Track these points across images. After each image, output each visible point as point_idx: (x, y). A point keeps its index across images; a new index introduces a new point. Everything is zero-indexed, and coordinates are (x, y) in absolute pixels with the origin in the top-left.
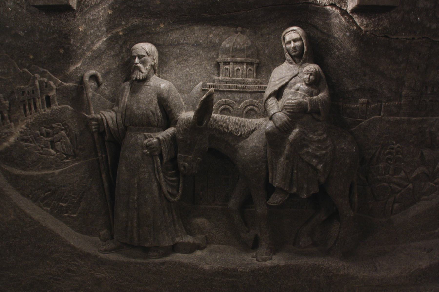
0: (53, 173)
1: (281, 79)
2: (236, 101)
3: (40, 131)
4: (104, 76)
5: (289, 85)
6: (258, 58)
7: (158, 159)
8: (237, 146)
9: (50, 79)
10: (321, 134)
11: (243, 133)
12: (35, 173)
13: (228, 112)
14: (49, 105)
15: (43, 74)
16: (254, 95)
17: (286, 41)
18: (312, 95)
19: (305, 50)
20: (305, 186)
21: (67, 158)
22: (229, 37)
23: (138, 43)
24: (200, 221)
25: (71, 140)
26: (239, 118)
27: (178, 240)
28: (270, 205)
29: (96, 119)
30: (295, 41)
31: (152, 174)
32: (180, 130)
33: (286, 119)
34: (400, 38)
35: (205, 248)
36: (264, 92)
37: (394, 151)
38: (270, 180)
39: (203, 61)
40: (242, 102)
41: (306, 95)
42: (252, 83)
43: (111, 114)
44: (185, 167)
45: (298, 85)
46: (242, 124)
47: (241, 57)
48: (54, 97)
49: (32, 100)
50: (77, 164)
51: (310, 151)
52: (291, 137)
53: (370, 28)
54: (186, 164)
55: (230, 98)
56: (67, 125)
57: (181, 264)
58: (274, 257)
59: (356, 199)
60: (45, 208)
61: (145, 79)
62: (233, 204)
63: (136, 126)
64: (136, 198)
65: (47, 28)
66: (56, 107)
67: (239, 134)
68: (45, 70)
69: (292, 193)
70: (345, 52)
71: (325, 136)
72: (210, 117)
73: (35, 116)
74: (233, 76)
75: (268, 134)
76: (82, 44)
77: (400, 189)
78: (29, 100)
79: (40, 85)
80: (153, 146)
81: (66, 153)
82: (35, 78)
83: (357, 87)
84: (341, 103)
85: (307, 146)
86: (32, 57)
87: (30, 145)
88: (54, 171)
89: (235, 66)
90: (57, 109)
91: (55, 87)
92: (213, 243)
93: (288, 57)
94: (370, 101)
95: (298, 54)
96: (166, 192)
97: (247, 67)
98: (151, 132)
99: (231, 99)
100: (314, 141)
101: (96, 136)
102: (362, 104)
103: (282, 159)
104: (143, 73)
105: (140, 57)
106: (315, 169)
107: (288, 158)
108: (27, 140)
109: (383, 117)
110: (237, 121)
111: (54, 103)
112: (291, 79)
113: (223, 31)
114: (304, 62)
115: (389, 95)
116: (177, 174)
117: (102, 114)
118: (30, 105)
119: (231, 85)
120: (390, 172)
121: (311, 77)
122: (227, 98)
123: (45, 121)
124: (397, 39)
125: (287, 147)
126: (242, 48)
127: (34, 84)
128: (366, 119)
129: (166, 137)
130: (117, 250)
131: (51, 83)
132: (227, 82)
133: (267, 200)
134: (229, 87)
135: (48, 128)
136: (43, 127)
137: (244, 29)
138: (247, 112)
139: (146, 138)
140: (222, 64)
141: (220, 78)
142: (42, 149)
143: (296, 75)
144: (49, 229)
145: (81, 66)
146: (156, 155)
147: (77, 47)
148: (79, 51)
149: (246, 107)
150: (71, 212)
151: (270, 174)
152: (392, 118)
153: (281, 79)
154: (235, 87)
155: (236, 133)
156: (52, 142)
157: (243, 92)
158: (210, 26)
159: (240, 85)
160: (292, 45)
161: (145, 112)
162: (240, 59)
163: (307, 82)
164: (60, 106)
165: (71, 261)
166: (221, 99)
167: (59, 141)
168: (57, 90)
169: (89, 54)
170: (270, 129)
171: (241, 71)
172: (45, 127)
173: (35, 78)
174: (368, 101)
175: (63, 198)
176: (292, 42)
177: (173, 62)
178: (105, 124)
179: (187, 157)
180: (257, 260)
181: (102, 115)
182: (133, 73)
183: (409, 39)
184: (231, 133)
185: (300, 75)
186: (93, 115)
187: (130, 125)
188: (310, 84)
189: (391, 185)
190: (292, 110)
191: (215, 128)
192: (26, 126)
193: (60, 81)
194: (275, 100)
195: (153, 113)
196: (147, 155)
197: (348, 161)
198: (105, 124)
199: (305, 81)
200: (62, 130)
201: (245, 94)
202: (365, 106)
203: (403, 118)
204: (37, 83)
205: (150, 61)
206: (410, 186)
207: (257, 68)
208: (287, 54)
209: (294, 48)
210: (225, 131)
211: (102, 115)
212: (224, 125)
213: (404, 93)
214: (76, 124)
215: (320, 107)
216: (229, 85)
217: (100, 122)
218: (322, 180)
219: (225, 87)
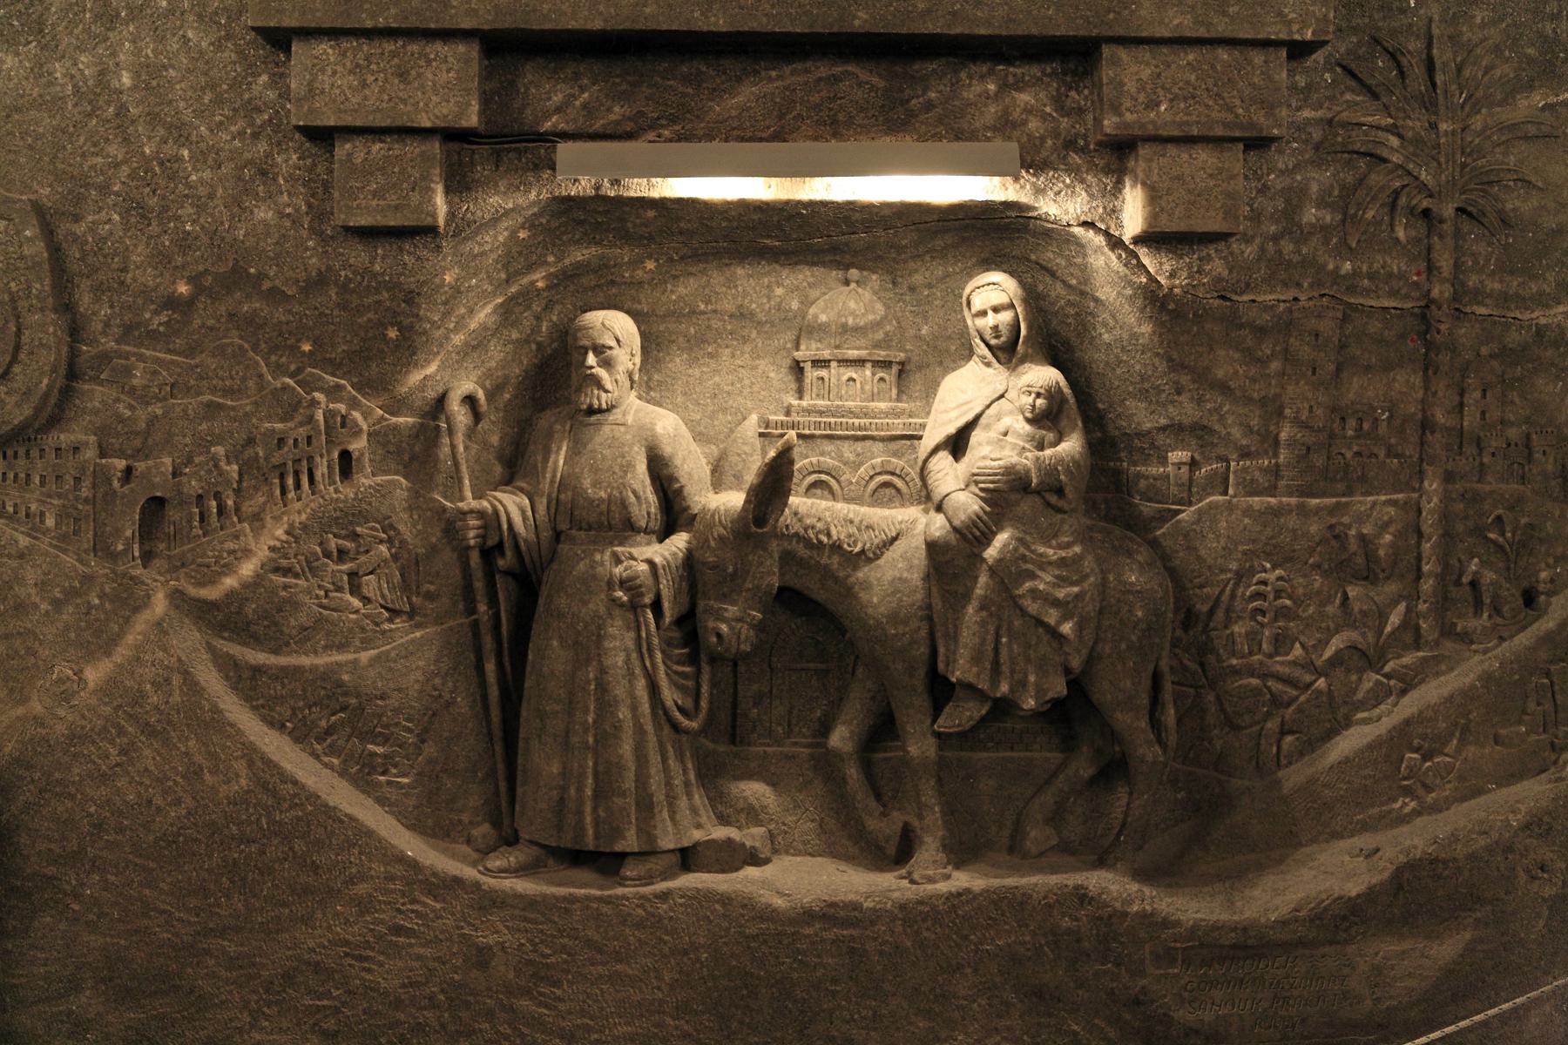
0: (355, 662)
1: (962, 404)
2: (845, 464)
3: (321, 544)
4: (491, 396)
5: (983, 421)
7: (650, 616)
8: (852, 579)
9: (354, 404)
10: (1068, 546)
11: (868, 545)
12: (306, 661)
13: (826, 493)
15: (334, 393)
16: (894, 445)
17: (974, 310)
18: (1041, 446)
19: (1023, 332)
20: (1032, 678)
21: (390, 620)
22: (825, 294)
24: (755, 790)
26: (857, 507)
27: (697, 835)
28: (943, 733)
29: (481, 514)
30: (996, 310)
31: (634, 655)
32: (707, 540)
33: (976, 507)
34: (1259, 299)
35: (767, 861)
36: (920, 438)
37: (1269, 588)
38: (941, 666)
39: (758, 357)
40: (861, 464)
41: (1027, 446)
42: (887, 415)
43: (517, 499)
44: (719, 636)
45: (1007, 421)
46: (865, 523)
47: (858, 349)
48: (362, 454)
49: (305, 463)
50: (418, 634)
51: (1041, 587)
52: (991, 553)
53: (1182, 280)
54: (724, 628)
55: (829, 454)
56: (395, 529)
58: (956, 874)
59: (1170, 716)
60: (326, 759)
62: (840, 738)
63: (590, 528)
64: (590, 720)
65: (363, 278)
66: (365, 480)
67: (857, 549)
68: (343, 382)
69: (998, 695)
70: (1126, 336)
71: (1077, 549)
72: (785, 504)
73: (312, 505)
75: (933, 548)
76: (446, 315)
77: (1295, 693)
79: (326, 421)
80: (638, 581)
81: (390, 606)
83: (1163, 421)
84: (1125, 464)
85: (1033, 576)
86: (307, 348)
87: (296, 585)
88: (356, 656)
89: (842, 370)
90: (370, 486)
91: (365, 428)
92: (787, 853)
93: (984, 351)
94: (1197, 456)
95: (1004, 343)
96: (669, 703)
97: (874, 374)
98: (631, 546)
99: (832, 458)
100: (1050, 563)
101: (475, 558)
102: (1179, 465)
103: (970, 610)
104: (607, 391)
106: (1054, 633)
107: (982, 608)
108: (287, 571)
109: (1235, 500)
110: (851, 515)
111: (362, 470)
112: (988, 406)
113: (811, 280)
114: (1022, 361)
115: (1244, 443)
116: (693, 659)
117: (495, 498)
118: (297, 474)
119: (832, 420)
120: (1264, 646)
121: (1040, 402)
122: (822, 454)
123: (337, 518)
124: (1254, 301)
125: (983, 579)
126: (862, 324)
127: (310, 419)
128: (1190, 504)
131: (356, 415)
132: (821, 413)
133: (934, 721)
135: (344, 538)
136: (331, 536)
137: (865, 273)
138: (875, 491)
139: (618, 561)
140: (808, 366)
141: (804, 403)
142: (326, 596)
143: (1002, 396)
144: (346, 815)
145: (438, 371)
146: (645, 606)
147: (433, 323)
149: (871, 477)
150: (394, 771)
151: (942, 650)
152: (1256, 501)
153: (962, 404)
154: (844, 427)
155: (849, 545)
156: (353, 575)
157: (865, 438)
158: (777, 267)
159: (856, 421)
160: (991, 319)
161: (616, 493)
162: (856, 352)
163: (1029, 415)
164: (379, 479)
165: (403, 904)
166: (807, 457)
168: (369, 435)
169: (458, 339)
170: (937, 534)
171: (858, 385)
172: (335, 536)
173: (314, 403)
174: (1192, 457)
175: (378, 729)
176: (990, 313)
177: (678, 360)
178: (505, 526)
179: (726, 610)
180: (913, 882)
181: (497, 504)
182: (579, 390)
183: (1284, 301)
184: (836, 547)
185: (1011, 395)
186: (470, 502)
187: (570, 529)
188: (1036, 420)
189: (1269, 684)
190: (991, 486)
191: (796, 534)
192: (288, 533)
194: (951, 458)
196: (622, 605)
197: (1140, 614)
198: (505, 526)
199: (1023, 413)
200: (381, 542)
201: (868, 443)
202: (1185, 469)
203: (1284, 499)
204: (319, 416)
206: (1321, 683)
207: (901, 372)
208: (978, 341)
209: (995, 328)
210: (820, 542)
211: (497, 504)
213: (1283, 436)
214: (420, 527)
215: (1062, 477)
216: (828, 420)
217: (490, 521)
218: (1076, 663)
219: (818, 425)
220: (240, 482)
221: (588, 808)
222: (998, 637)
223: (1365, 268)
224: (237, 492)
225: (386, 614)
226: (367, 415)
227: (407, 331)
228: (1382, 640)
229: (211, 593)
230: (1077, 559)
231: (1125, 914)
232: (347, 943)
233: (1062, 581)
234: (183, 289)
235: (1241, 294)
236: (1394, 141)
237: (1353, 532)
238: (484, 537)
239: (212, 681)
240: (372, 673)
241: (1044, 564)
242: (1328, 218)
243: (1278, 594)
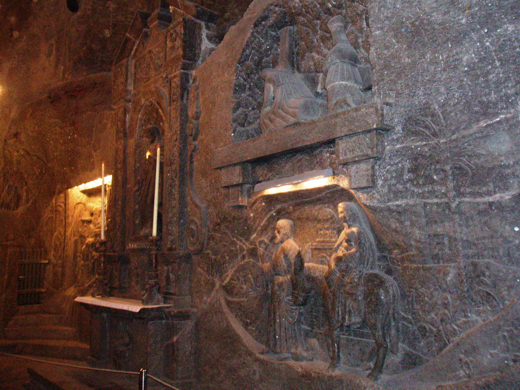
9: (244, 244)
30: (342, 212)
76: (255, 223)
131: (244, 246)
169: (259, 228)
204: (238, 246)
229: (224, 284)
235: (388, 202)
239: (223, 302)
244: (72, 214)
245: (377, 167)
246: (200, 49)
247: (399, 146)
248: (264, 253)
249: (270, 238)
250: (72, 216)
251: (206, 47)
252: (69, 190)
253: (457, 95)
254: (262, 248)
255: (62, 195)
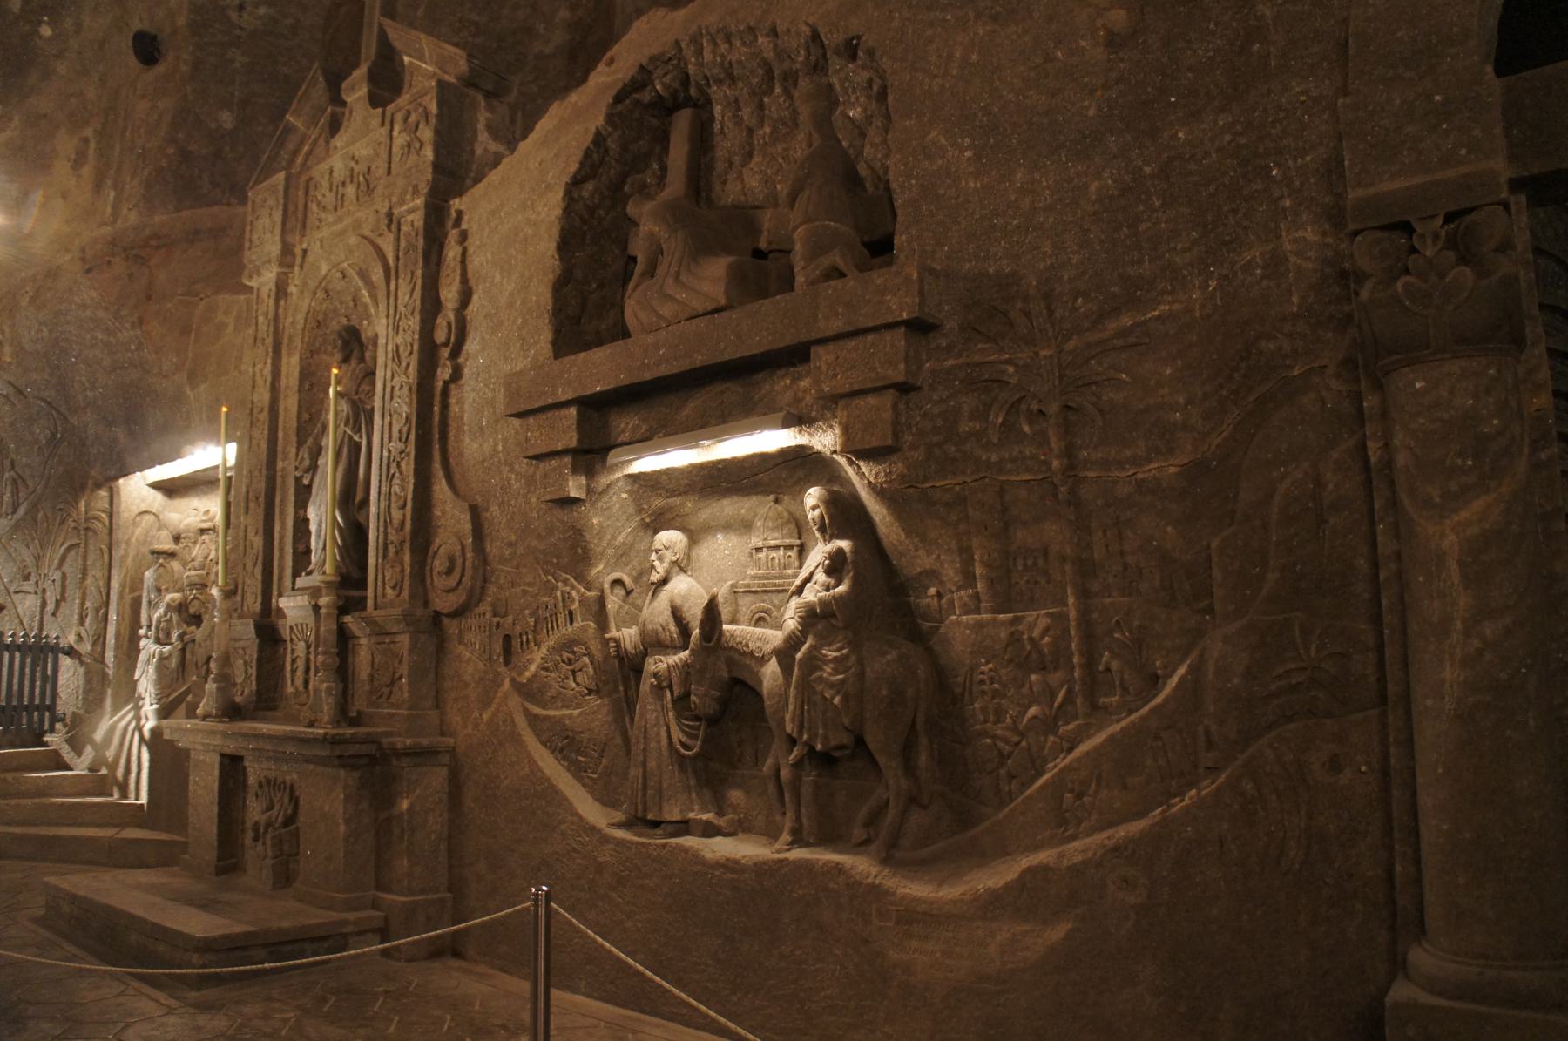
2: (774, 606)
6: (800, 538)
12: (552, 713)
14: (571, 622)
15: (565, 582)
19: (827, 521)
20: (821, 731)
21: (589, 694)
23: (663, 529)
25: (595, 669)
27: (692, 815)
29: (614, 639)
30: (814, 508)
34: (938, 485)
51: (825, 675)
52: (799, 655)
57: (686, 850)
61: (664, 581)
66: (578, 623)
71: (844, 651)
72: (721, 630)
74: (768, 568)
78: (551, 616)
82: (557, 588)
85: (822, 669)
91: (577, 598)
97: (785, 554)
103: (792, 689)
105: (657, 551)
107: (796, 688)
108: (547, 669)
122: (764, 601)
124: (933, 487)
129: (677, 661)
130: (625, 825)
131: (574, 593)
132: (760, 578)
134: (764, 585)
148: (599, 550)
167: (580, 670)
169: (611, 552)
173: (557, 588)
183: (958, 484)
184: (751, 653)
191: (732, 647)
193: (583, 590)
195: (664, 629)
200: (585, 655)
202: (936, 598)
204: (559, 593)
205: (669, 556)
212: (744, 642)
218: (846, 721)
220: (535, 626)
221: (640, 794)
222: (802, 708)
223: (1007, 456)
224: (534, 631)
225: (586, 691)
226: (577, 592)
227: (585, 549)
228: (1054, 710)
230: (845, 658)
231: (860, 884)
232: (557, 853)
233: (836, 671)
234: (513, 538)
235: (923, 483)
236: (1011, 369)
237: (1025, 637)
238: (618, 651)
239: (521, 721)
240: (578, 720)
241: (826, 662)
242: (978, 426)
243: (992, 680)
244: (126, 537)
245: (902, 407)
246: (473, 152)
247: (950, 362)
248: (621, 607)
249: (634, 573)
250: (128, 543)
251: (486, 150)
252: (121, 481)
253: (1075, 259)
254: (616, 596)
255: (104, 493)
